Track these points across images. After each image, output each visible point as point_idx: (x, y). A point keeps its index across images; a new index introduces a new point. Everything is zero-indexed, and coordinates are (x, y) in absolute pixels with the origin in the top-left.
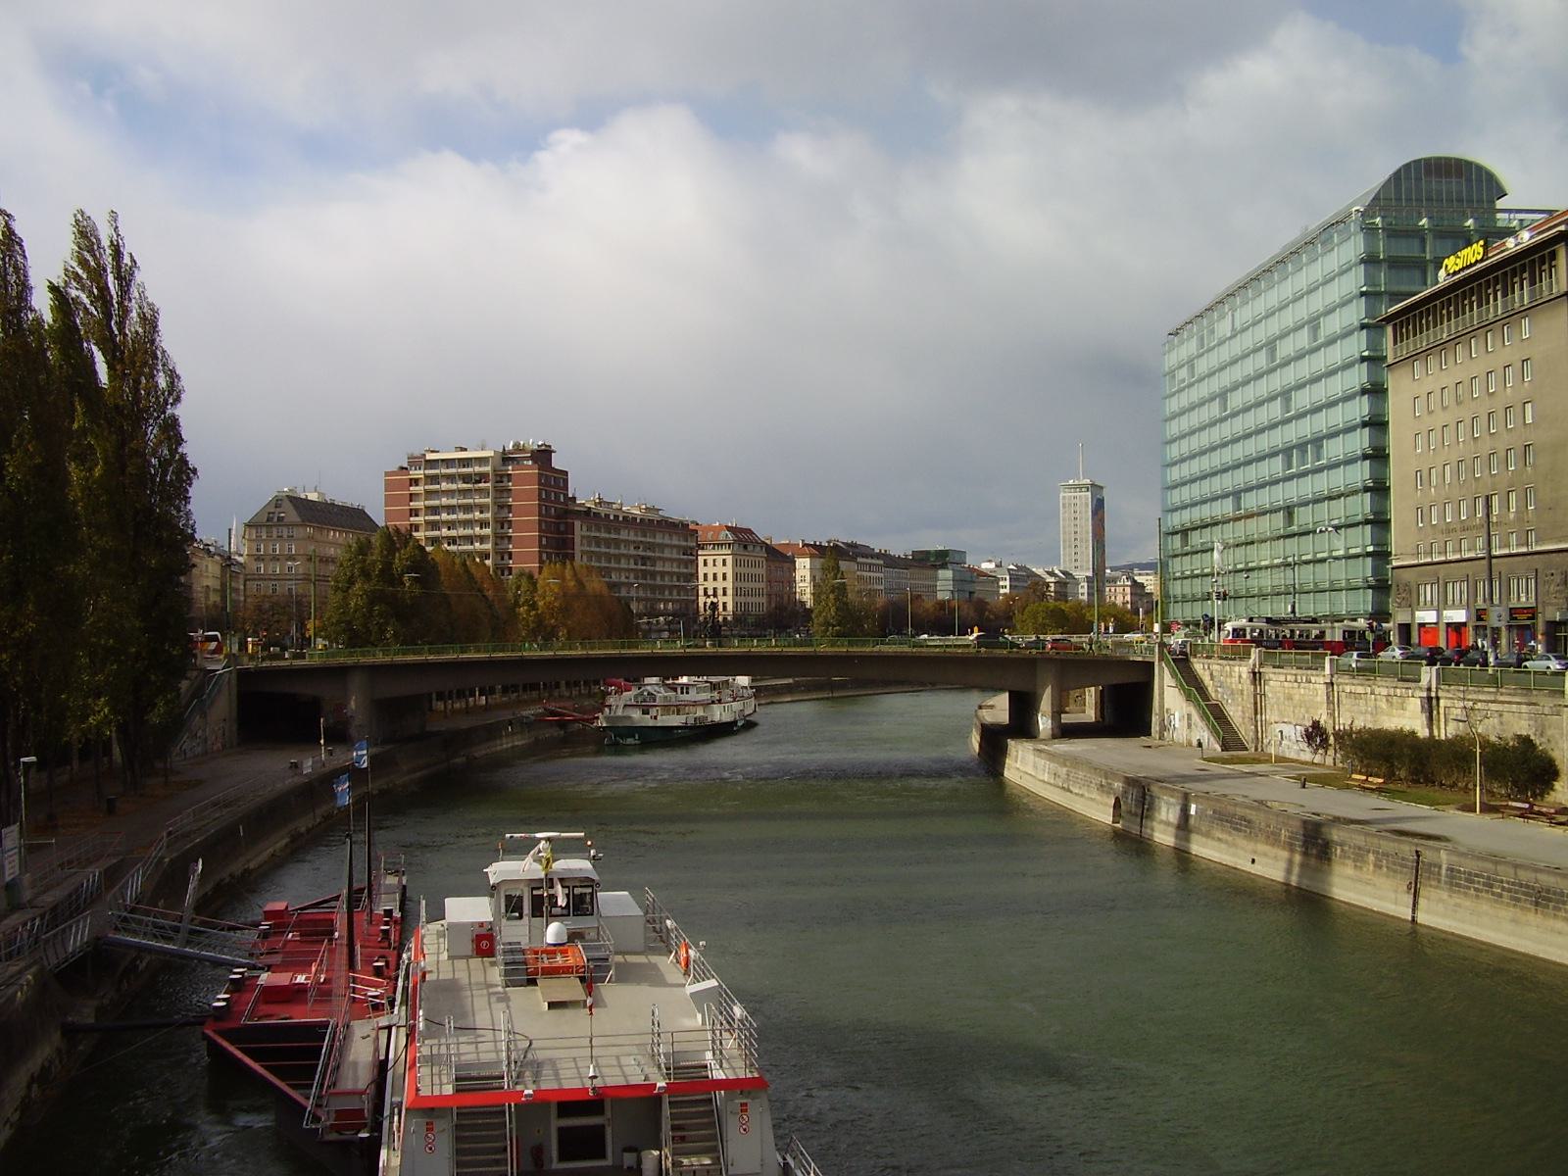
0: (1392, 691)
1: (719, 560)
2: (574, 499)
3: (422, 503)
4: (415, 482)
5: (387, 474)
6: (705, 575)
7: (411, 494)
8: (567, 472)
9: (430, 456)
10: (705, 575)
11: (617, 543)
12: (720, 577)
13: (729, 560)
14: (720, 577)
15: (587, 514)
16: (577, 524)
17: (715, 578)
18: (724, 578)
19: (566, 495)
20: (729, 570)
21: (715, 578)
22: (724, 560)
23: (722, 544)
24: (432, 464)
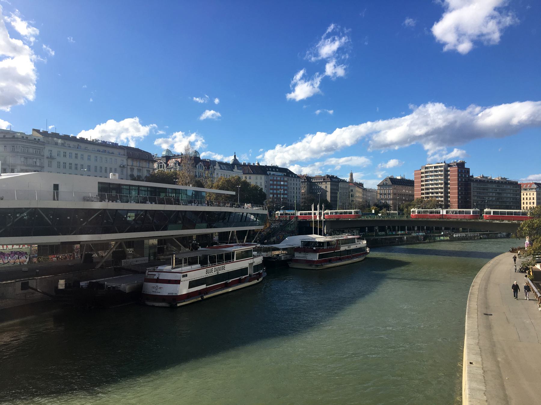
1: (532, 193)
2: (472, 176)
3: (424, 179)
5: (415, 171)
8: (469, 169)
9: (426, 166)
12: (532, 199)
13: (535, 193)
14: (532, 199)
15: (477, 181)
16: (472, 183)
18: (533, 199)
20: (535, 196)
23: (533, 189)
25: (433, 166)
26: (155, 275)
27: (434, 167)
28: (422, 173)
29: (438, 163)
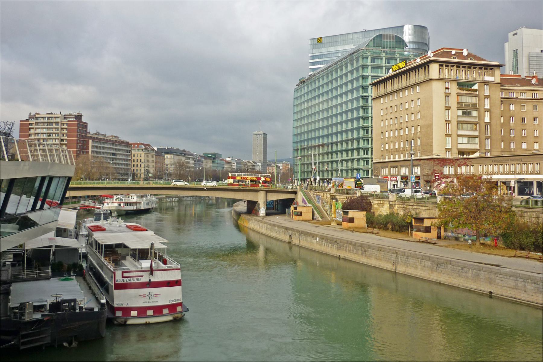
0: (379, 202)
4: (31, 124)
5: (21, 121)
6: (134, 160)
7: (30, 129)
9: (37, 116)
10: (134, 160)
11: (103, 148)
13: (143, 155)
16: (90, 141)
17: (137, 161)
19: (86, 131)
21: (137, 161)
22: (141, 155)
24: (37, 118)
25: (46, 117)
26: (142, 276)
27: (47, 118)
28: (31, 124)
29: (49, 114)
